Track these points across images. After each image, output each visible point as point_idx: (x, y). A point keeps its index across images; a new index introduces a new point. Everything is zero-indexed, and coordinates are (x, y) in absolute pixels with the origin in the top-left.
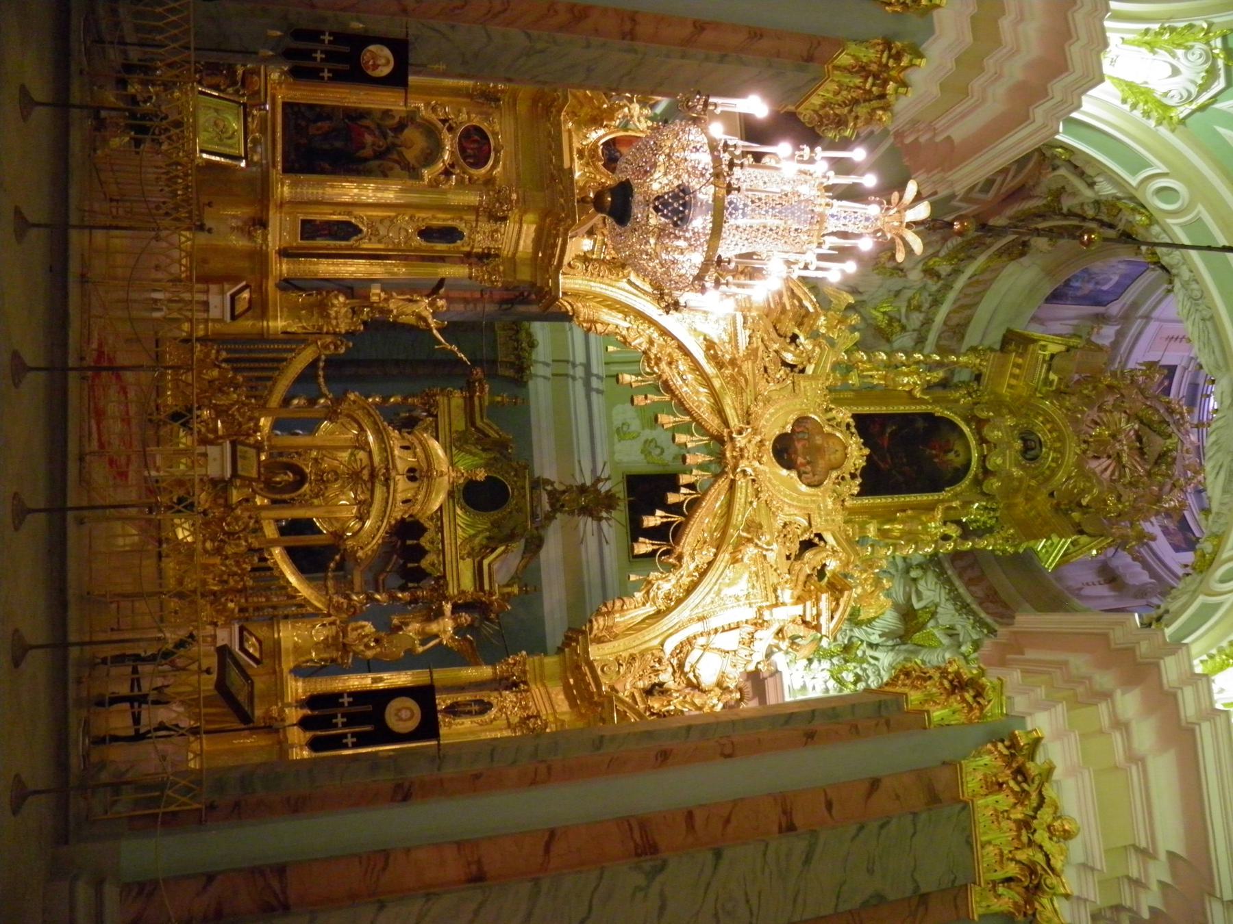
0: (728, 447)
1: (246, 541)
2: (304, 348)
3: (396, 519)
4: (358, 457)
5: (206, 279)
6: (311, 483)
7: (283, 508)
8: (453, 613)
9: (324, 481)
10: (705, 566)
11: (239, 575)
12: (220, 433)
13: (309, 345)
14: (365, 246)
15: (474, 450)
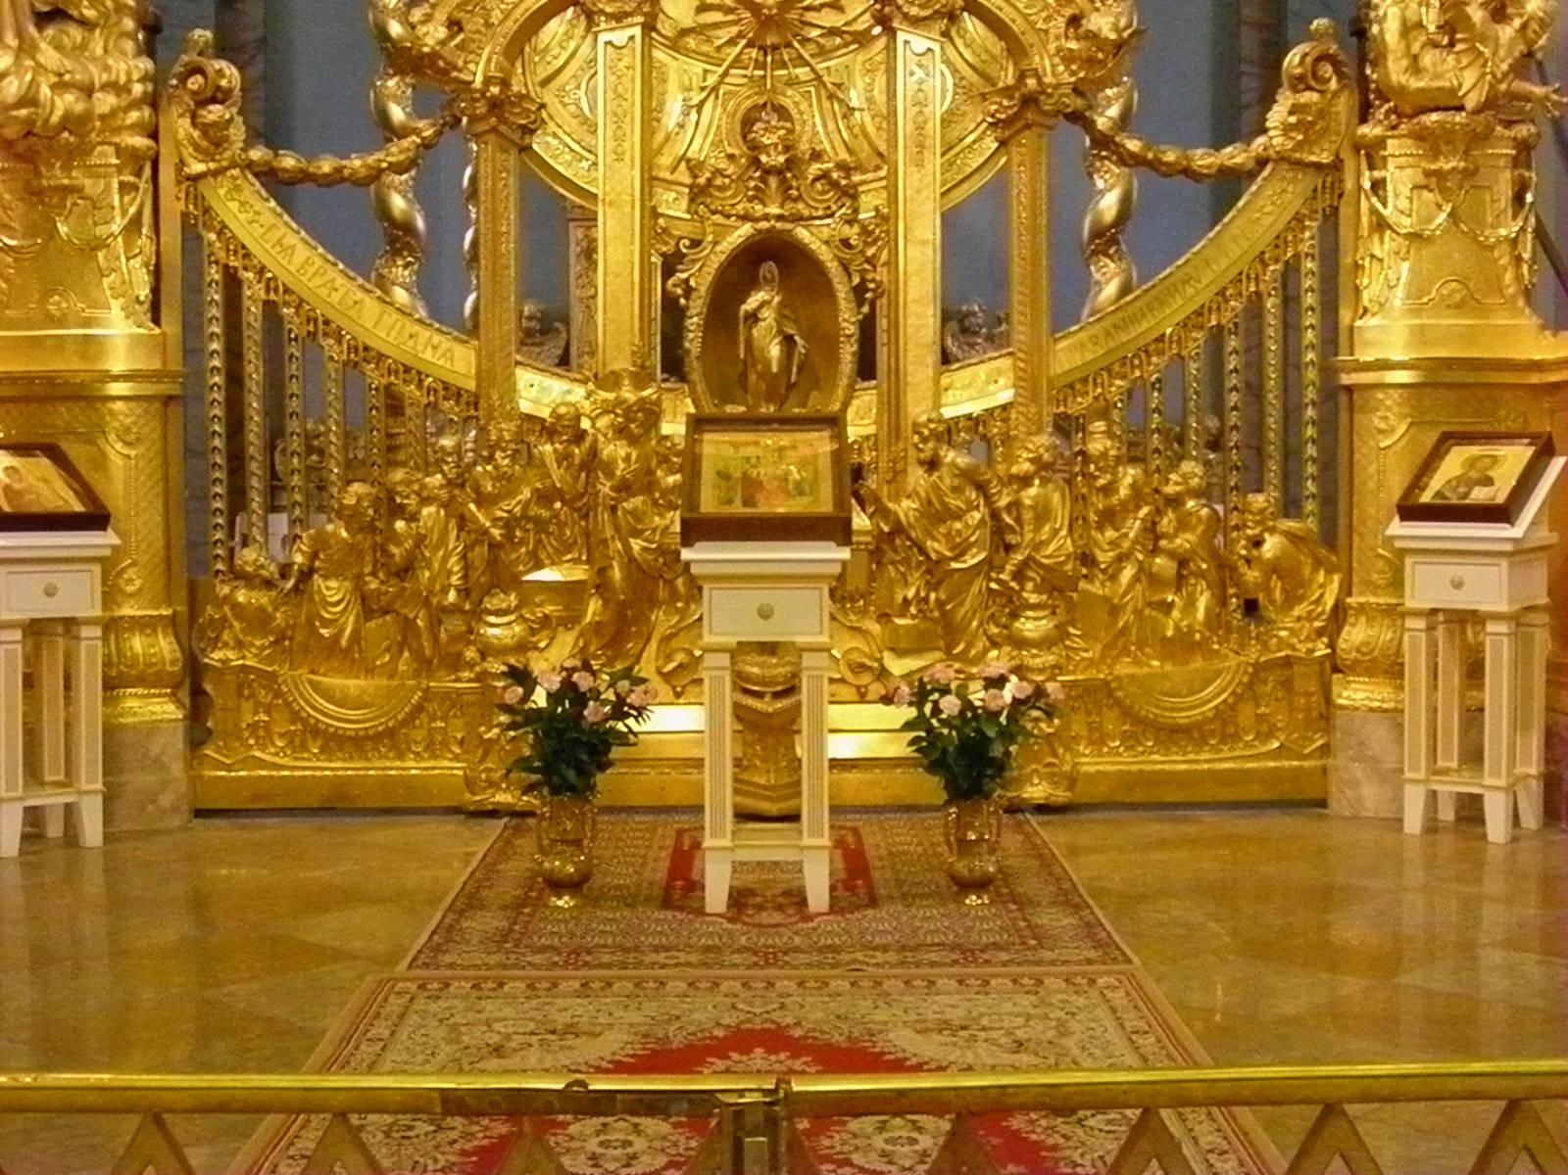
1: (1025, 481)
2: (222, 230)
4: (688, 22)
6: (798, 219)
7: (894, 325)
9: (790, 164)
11: (1159, 512)
12: (579, 573)
13: (207, 210)
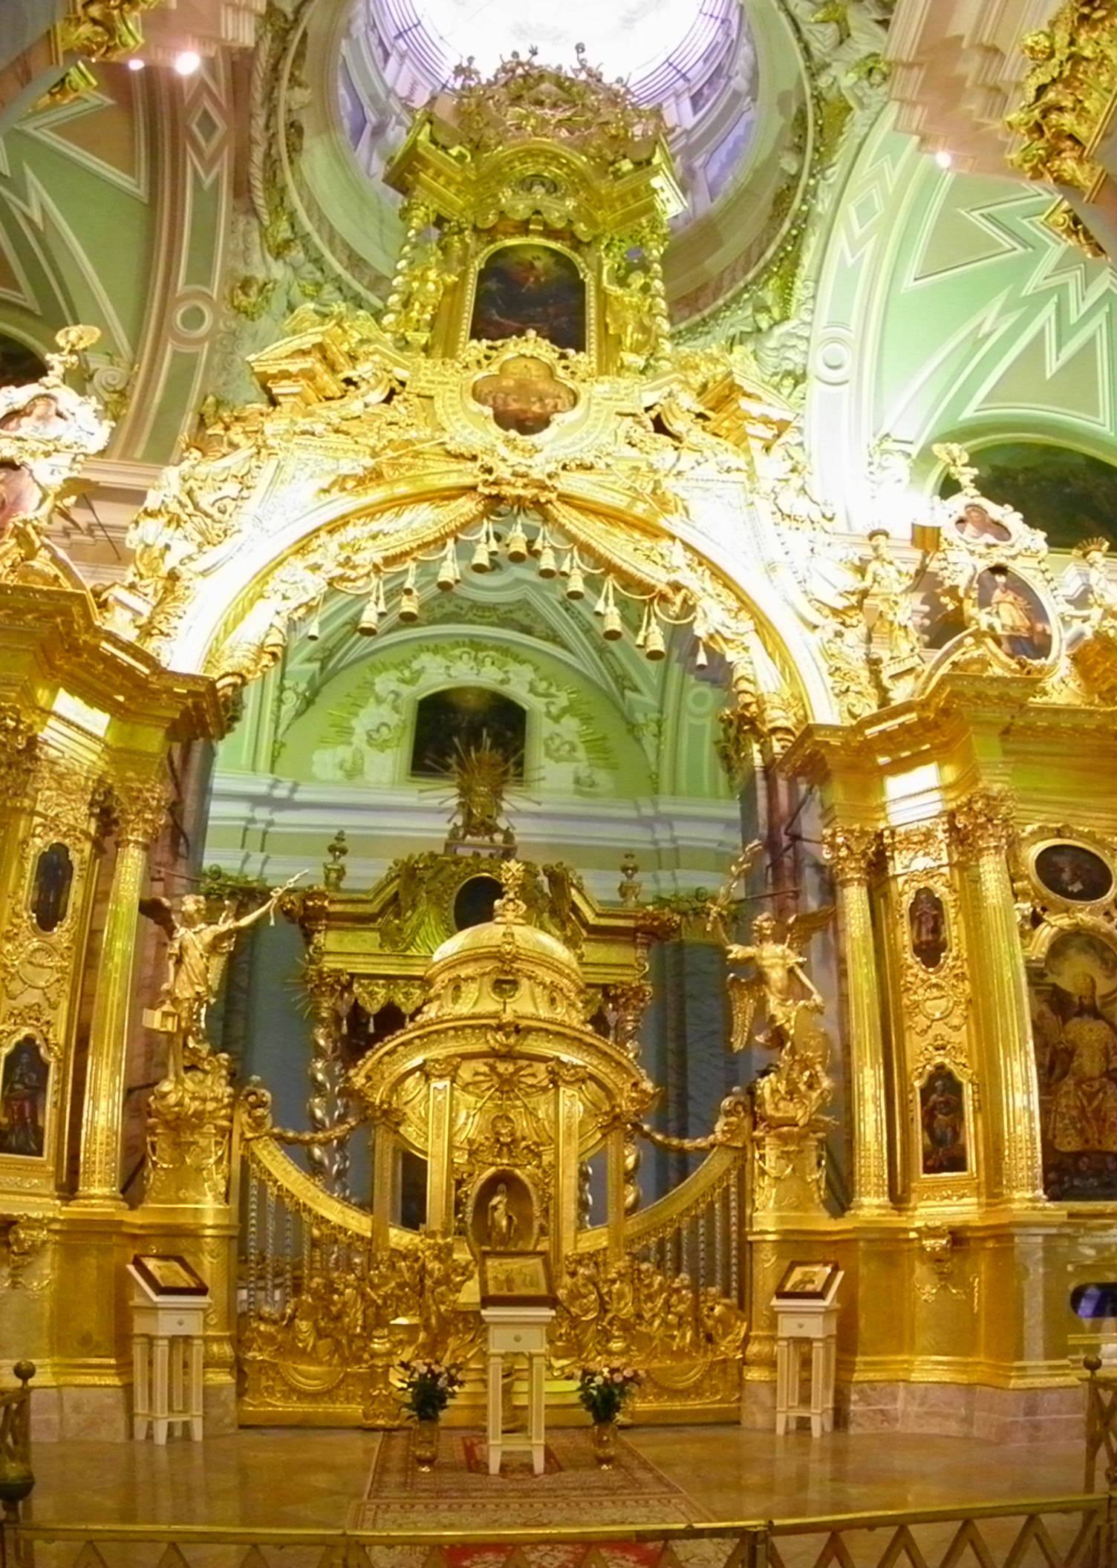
0: (507, 491)
3: (585, 1022)
5: (121, 1341)
8: (747, 943)
10: (689, 555)
14: (61, 1039)
15: (414, 921)
